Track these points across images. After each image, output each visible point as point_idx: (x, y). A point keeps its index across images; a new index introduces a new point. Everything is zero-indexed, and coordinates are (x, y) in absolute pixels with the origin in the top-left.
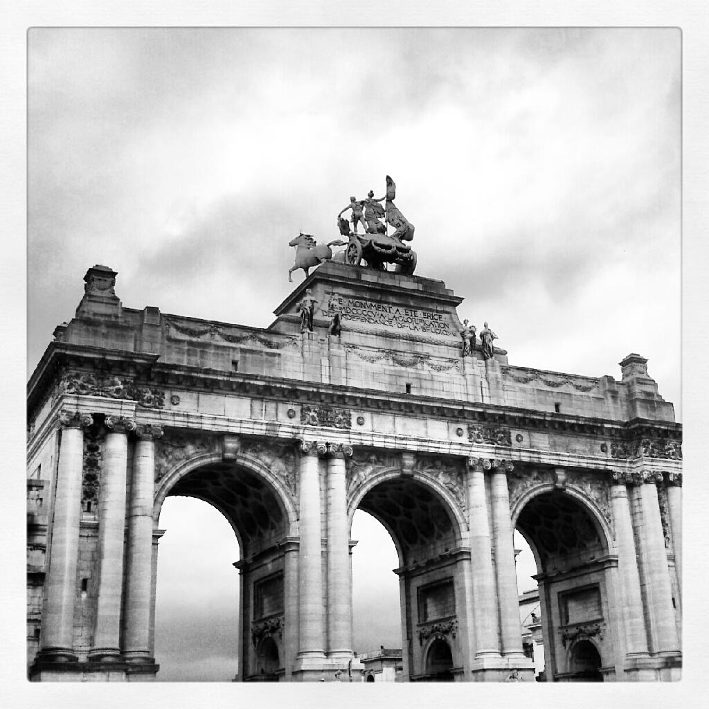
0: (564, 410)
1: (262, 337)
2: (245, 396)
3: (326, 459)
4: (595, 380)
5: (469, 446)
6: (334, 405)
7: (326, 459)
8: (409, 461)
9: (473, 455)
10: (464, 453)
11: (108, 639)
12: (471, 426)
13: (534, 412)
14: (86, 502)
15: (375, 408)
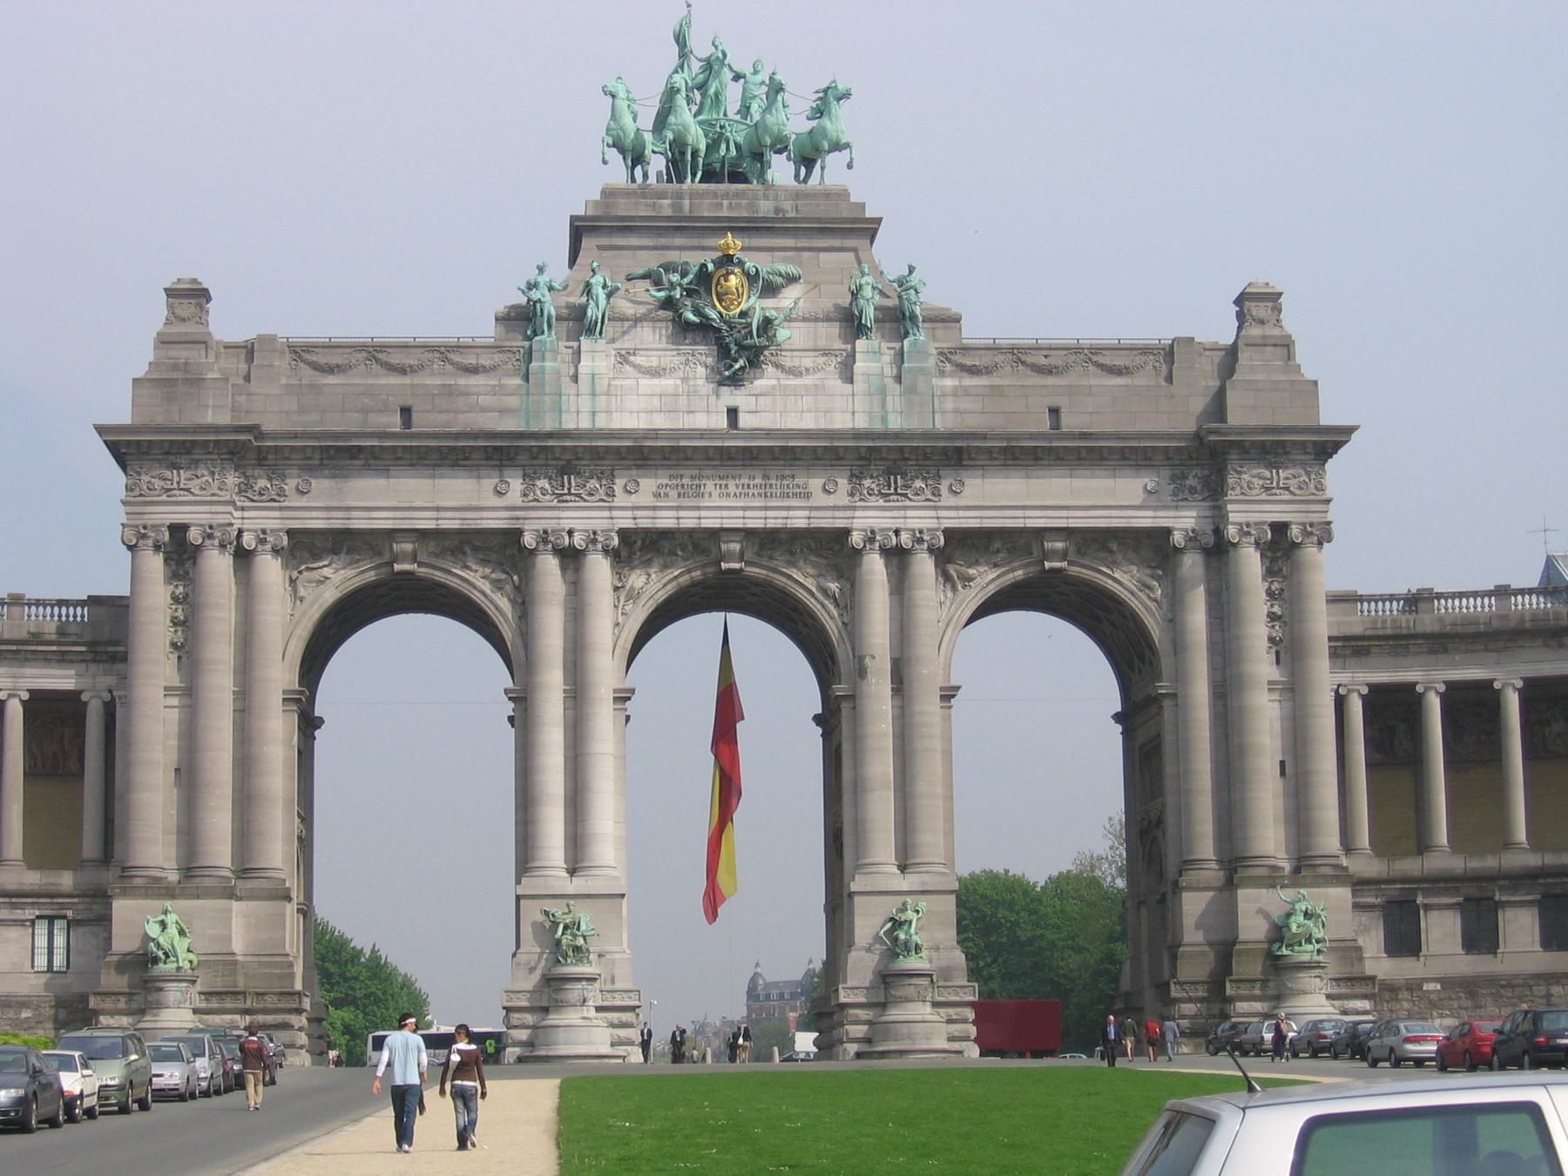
0: (1069, 423)
1: (456, 358)
2: (424, 465)
3: (571, 558)
4: (1145, 350)
5: (845, 508)
6: (583, 463)
7: (571, 558)
8: (736, 547)
9: (857, 524)
10: (840, 524)
11: (220, 852)
12: (856, 472)
13: (984, 437)
14: (176, 655)
15: (659, 459)
